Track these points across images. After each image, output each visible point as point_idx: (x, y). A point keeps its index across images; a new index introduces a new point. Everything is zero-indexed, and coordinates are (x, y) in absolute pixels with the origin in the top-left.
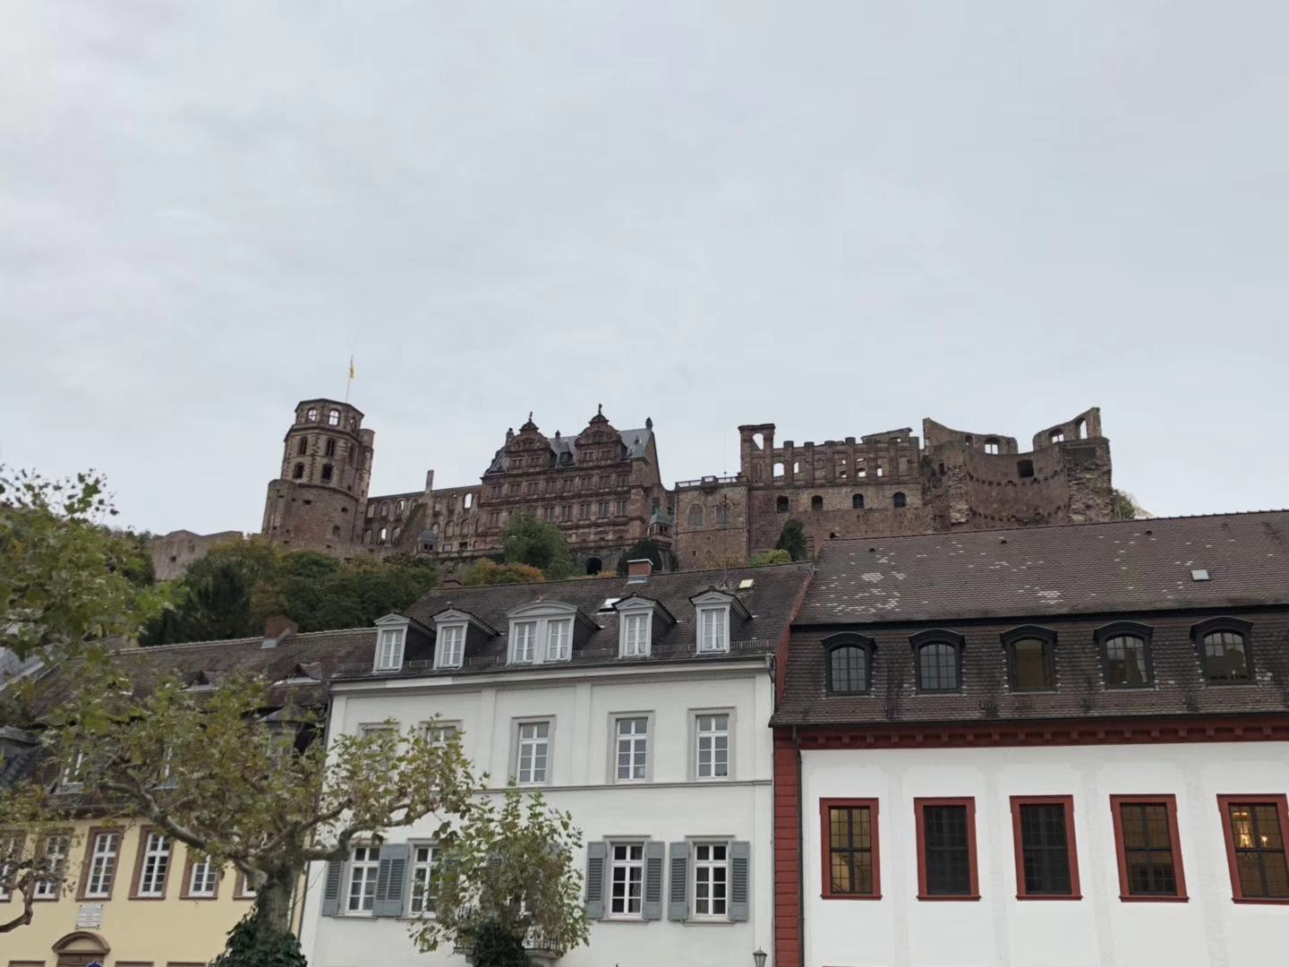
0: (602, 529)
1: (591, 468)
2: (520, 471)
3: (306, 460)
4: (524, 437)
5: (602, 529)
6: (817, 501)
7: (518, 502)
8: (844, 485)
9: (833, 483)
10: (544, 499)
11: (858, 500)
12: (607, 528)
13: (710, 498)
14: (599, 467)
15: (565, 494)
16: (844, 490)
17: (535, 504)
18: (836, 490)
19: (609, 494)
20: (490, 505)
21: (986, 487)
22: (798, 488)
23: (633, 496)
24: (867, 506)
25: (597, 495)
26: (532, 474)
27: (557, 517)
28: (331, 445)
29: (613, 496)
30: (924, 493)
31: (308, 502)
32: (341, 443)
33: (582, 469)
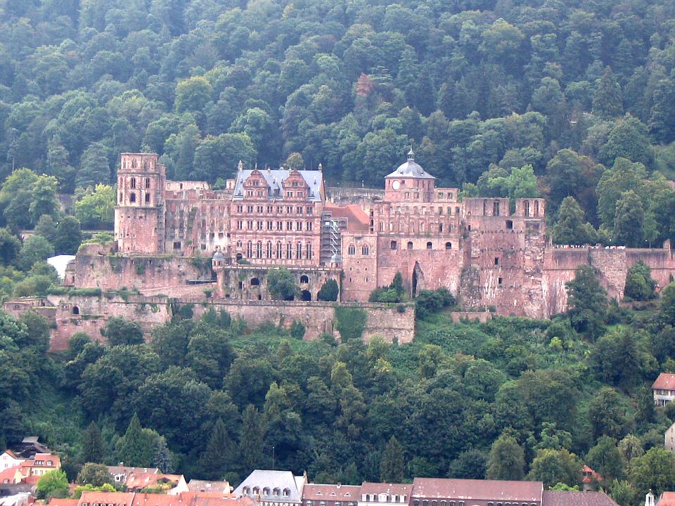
0: (298, 237)
1: (292, 202)
2: (252, 199)
3: (136, 192)
4: (253, 178)
5: (298, 237)
6: (410, 244)
7: (252, 217)
8: (422, 236)
9: (418, 236)
10: (267, 217)
11: (429, 244)
12: (302, 236)
13: (359, 242)
14: (296, 202)
15: (278, 215)
16: (423, 240)
17: (262, 219)
18: (419, 240)
19: (302, 217)
20: (236, 216)
21: (490, 234)
22: (402, 236)
23: (316, 222)
24: (433, 249)
25: (296, 217)
26: (260, 201)
27: (274, 228)
28: (148, 181)
29: (304, 220)
30: (460, 242)
31: (141, 217)
32: (152, 180)
33: (286, 202)
